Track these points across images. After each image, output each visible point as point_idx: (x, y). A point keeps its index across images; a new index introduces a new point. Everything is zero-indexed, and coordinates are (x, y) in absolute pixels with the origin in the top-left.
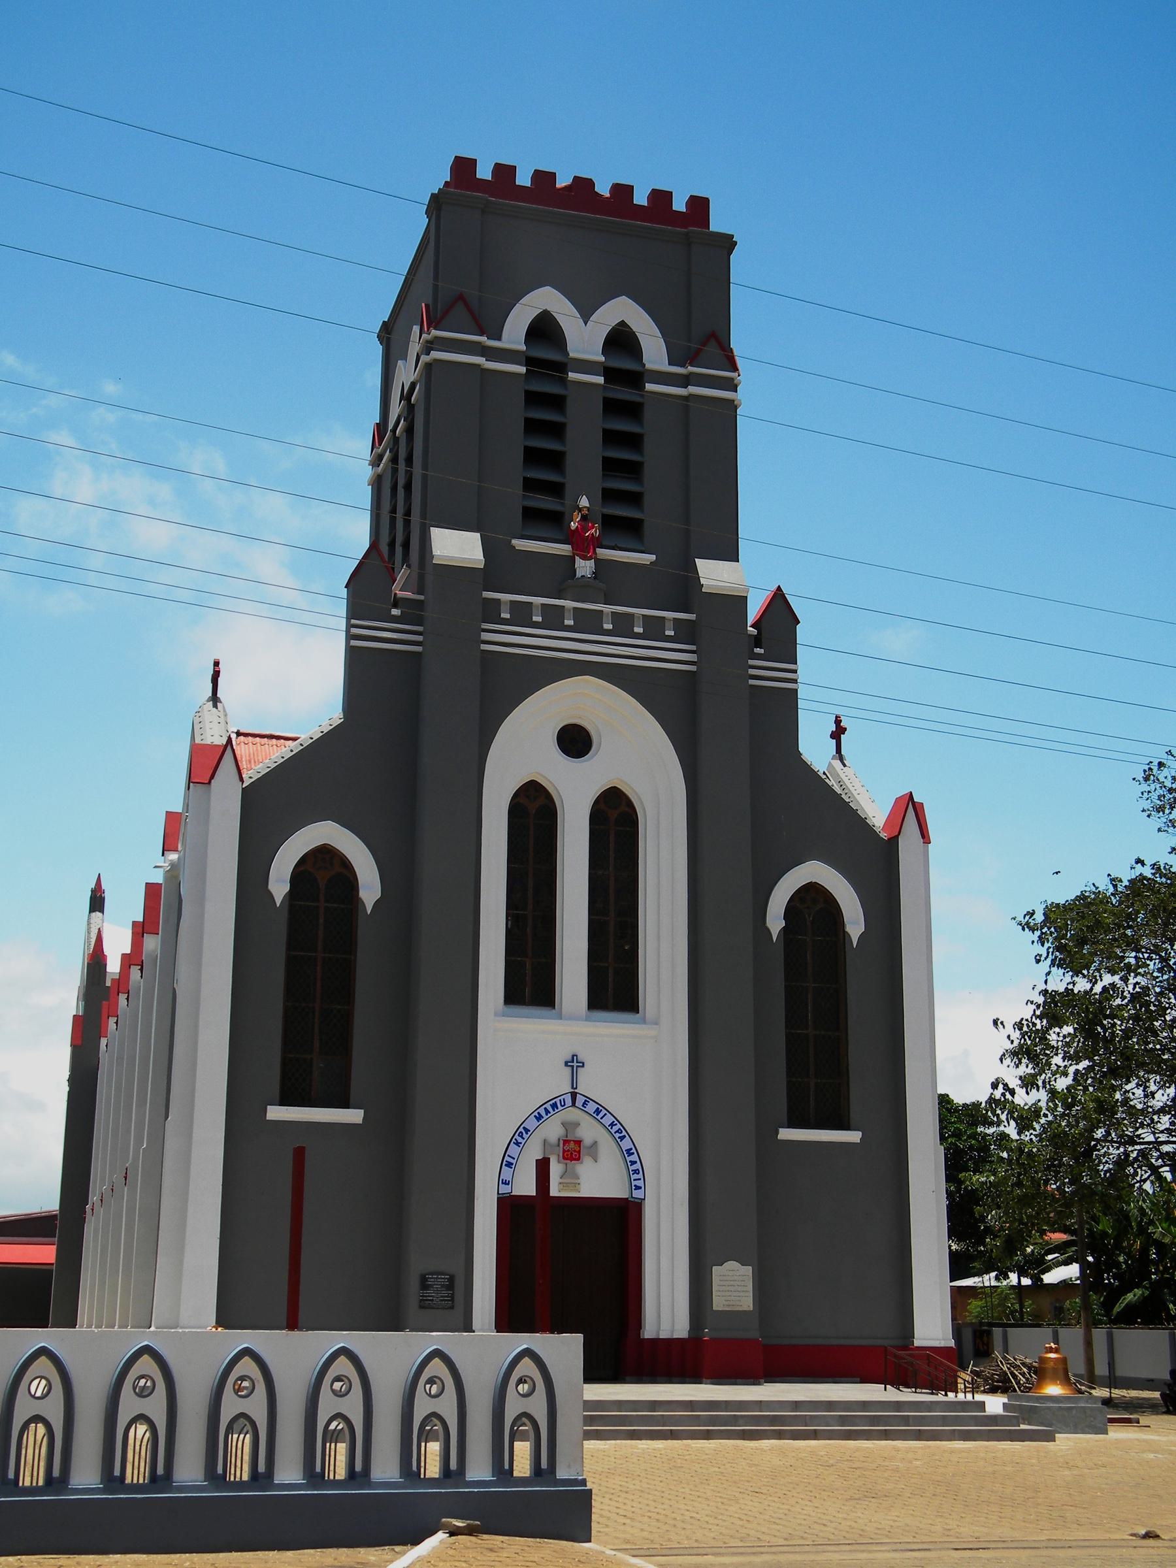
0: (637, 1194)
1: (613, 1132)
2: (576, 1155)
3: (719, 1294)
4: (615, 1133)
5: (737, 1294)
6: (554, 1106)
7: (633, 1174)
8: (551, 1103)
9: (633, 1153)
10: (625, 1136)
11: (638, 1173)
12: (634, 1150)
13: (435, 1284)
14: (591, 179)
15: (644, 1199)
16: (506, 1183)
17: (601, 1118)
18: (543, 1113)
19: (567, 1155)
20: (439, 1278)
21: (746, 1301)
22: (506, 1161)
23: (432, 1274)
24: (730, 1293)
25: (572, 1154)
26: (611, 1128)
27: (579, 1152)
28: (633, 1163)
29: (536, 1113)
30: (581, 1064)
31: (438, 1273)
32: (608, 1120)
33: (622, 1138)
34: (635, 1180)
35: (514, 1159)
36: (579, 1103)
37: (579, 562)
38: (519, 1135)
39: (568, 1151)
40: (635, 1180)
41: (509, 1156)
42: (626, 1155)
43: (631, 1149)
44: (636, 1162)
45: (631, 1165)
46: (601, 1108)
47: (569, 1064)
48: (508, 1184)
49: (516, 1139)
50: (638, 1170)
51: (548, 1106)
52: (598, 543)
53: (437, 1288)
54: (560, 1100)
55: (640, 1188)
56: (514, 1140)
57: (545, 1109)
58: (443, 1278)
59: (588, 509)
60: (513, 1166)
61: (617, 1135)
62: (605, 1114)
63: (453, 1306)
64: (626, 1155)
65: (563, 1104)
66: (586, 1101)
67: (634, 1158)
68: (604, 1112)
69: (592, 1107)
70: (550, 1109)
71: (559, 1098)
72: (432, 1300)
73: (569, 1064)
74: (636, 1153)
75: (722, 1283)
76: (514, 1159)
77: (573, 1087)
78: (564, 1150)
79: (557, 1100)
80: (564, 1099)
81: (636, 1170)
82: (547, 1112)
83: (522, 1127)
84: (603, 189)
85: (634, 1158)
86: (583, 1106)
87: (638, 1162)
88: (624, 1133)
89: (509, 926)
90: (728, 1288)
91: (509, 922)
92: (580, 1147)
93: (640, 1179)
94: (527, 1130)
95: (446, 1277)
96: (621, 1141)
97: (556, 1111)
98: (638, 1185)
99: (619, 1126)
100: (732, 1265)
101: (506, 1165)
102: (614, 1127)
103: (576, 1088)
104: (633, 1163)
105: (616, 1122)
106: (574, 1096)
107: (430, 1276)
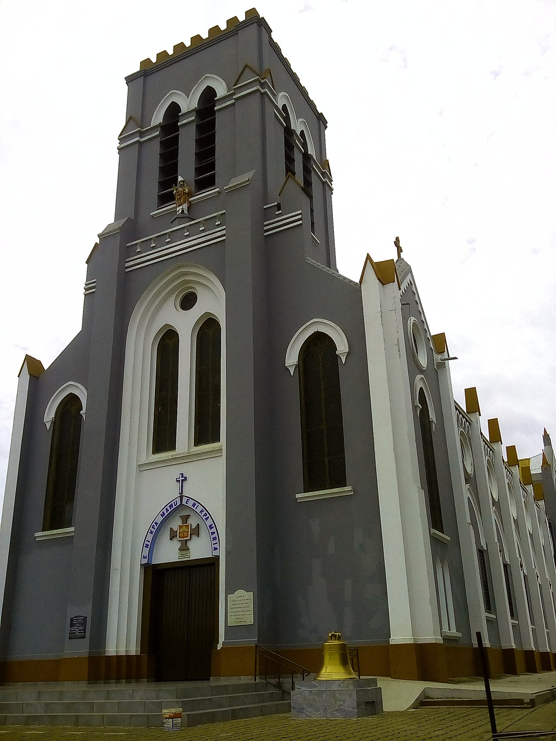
0: (216, 553)
2: (186, 534)
4: (203, 516)
5: (243, 613)
7: (213, 540)
8: (169, 505)
9: (213, 527)
13: (77, 623)
14: (198, 35)
15: (219, 556)
17: (196, 509)
19: (181, 535)
20: (79, 619)
21: (249, 618)
25: (184, 534)
26: (201, 514)
28: (213, 533)
29: (161, 513)
30: (184, 478)
33: (207, 519)
34: (214, 544)
35: (149, 542)
36: (184, 503)
38: (152, 527)
41: (147, 541)
43: (212, 525)
44: (214, 533)
45: (212, 535)
46: (196, 502)
47: (178, 479)
48: (146, 558)
49: (151, 530)
50: (216, 537)
51: (168, 507)
52: (190, 195)
53: (78, 625)
54: (174, 502)
55: (217, 549)
56: (150, 531)
57: (166, 509)
59: (183, 182)
60: (149, 547)
62: (198, 506)
63: (85, 636)
65: (176, 504)
66: (188, 500)
68: (197, 504)
69: (190, 504)
70: (169, 509)
71: (174, 501)
72: (75, 633)
73: (178, 479)
74: (214, 527)
75: (233, 606)
76: (149, 542)
77: (180, 493)
80: (176, 501)
81: (214, 538)
82: (167, 510)
85: (214, 530)
87: (216, 532)
88: (208, 515)
92: (188, 529)
93: (217, 543)
94: (156, 523)
95: (82, 618)
96: (206, 521)
97: (172, 509)
99: (205, 512)
102: (202, 513)
103: (182, 494)
104: (213, 533)
106: (181, 497)
107: (75, 619)
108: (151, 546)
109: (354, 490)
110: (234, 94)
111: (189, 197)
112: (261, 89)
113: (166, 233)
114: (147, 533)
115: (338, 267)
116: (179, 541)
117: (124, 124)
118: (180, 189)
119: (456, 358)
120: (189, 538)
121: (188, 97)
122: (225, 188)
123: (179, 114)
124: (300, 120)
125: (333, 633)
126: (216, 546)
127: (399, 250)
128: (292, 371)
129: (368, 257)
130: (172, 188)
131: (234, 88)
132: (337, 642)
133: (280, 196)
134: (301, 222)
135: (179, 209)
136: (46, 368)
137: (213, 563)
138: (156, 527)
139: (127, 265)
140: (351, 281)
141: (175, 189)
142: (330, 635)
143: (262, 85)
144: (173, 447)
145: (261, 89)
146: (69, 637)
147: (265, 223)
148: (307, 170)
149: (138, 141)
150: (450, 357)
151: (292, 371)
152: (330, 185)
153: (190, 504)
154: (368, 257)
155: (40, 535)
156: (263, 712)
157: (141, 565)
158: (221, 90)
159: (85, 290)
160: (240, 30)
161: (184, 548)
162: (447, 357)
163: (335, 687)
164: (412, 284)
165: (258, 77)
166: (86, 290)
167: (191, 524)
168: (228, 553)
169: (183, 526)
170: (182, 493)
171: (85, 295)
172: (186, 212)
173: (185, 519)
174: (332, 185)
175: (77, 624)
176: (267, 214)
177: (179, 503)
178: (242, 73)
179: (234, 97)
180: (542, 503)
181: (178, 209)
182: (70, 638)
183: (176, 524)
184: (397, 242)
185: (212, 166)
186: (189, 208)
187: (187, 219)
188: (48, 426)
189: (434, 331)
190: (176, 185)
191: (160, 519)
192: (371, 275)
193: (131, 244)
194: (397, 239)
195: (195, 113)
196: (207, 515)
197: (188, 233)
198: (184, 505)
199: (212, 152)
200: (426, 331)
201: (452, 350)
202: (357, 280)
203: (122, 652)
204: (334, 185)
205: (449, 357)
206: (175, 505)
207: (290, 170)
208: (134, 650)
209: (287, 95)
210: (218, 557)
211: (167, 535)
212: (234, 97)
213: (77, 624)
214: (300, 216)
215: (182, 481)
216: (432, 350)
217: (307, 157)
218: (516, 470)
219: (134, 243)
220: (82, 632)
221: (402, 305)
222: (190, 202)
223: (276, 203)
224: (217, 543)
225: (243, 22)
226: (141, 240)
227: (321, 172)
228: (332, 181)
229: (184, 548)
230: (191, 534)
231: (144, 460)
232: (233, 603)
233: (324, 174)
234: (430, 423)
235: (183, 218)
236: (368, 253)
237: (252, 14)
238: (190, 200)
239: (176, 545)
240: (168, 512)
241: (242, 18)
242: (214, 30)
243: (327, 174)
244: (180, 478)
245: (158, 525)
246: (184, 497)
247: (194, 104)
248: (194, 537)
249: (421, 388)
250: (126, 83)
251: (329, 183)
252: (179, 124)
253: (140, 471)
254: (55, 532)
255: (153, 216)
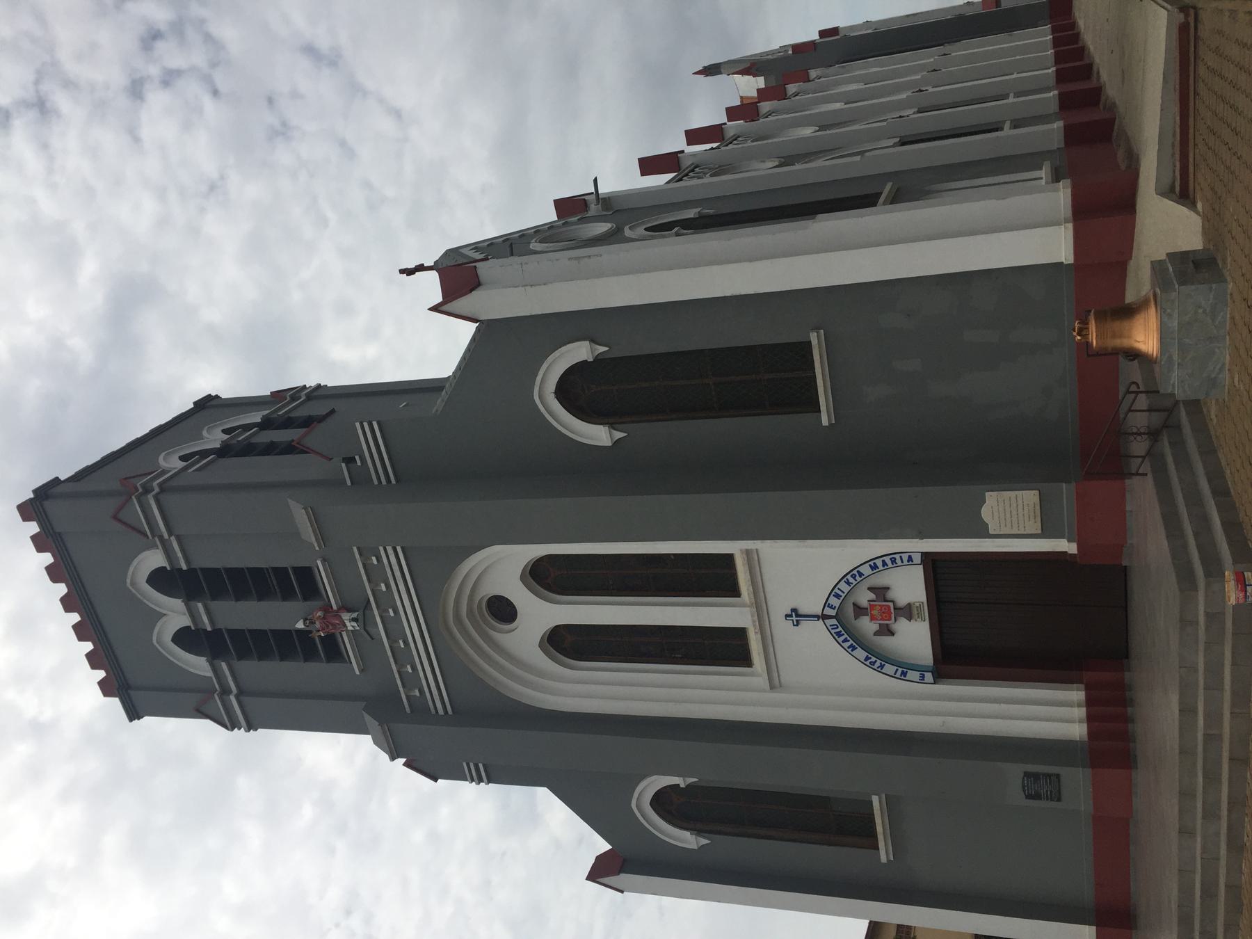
0: (917, 558)
1: (855, 583)
3: (1021, 526)
6: (839, 634)
7: (896, 563)
8: (836, 637)
9: (874, 563)
10: (858, 572)
11: (895, 559)
12: (871, 563)
15: (923, 554)
16: (923, 677)
17: (844, 593)
18: (847, 644)
19: (886, 617)
20: (1028, 784)
21: (1029, 498)
22: (901, 676)
23: (1024, 792)
24: (1020, 515)
27: (880, 605)
28: (884, 564)
29: (850, 650)
30: (794, 614)
31: (1023, 787)
32: (845, 587)
33: (861, 574)
34: (902, 562)
35: (897, 670)
36: (833, 613)
37: (350, 628)
38: (874, 665)
39: (881, 615)
40: (902, 562)
41: (895, 674)
42: (877, 570)
43: (870, 565)
44: (883, 561)
46: (833, 593)
47: (795, 624)
50: (891, 559)
51: (840, 640)
52: (327, 608)
56: (879, 669)
57: (843, 642)
58: (1028, 782)
59: (305, 620)
60: (905, 670)
61: (858, 578)
62: (839, 589)
64: (877, 570)
66: (828, 606)
67: (879, 563)
68: (836, 590)
69: (835, 602)
70: (843, 638)
71: (830, 629)
72: (1051, 792)
75: (1009, 525)
76: (897, 670)
77: (818, 620)
78: (881, 620)
79: (833, 631)
82: (845, 641)
83: (865, 663)
84: (62, 589)
85: (879, 563)
86: (834, 609)
88: (855, 572)
89: (680, 656)
90: (1015, 519)
91: (676, 656)
92: (876, 605)
93: (901, 557)
94: (867, 659)
97: (843, 632)
98: (907, 558)
99: (849, 577)
100: (986, 513)
101: (905, 676)
102: (850, 581)
104: (884, 564)
105: (845, 579)
106: (824, 617)
108: (904, 668)
109: (817, 329)
110: (161, 537)
111: (330, 610)
112: (154, 493)
113: (391, 647)
114: (883, 673)
115: (445, 375)
116: (895, 620)
117: (208, 722)
118: (318, 625)
119: (595, 180)
120: (891, 605)
121: (165, 615)
122: (317, 549)
123: (193, 628)
124: (205, 433)
125: (1075, 334)
126: (905, 557)
127: (421, 268)
128: (619, 435)
129: (435, 309)
130: (313, 640)
131: (151, 538)
132: (1092, 326)
133: (331, 459)
134: (375, 424)
135: (350, 626)
136: (611, 847)
137: (932, 563)
138: (873, 659)
139: (441, 712)
140: (473, 339)
141: (318, 634)
142: (1079, 338)
143: (147, 490)
144: (741, 633)
145: (154, 493)
146: (1057, 801)
147: (376, 482)
148: (288, 423)
149: (237, 697)
150: (593, 190)
151: (619, 435)
152: (311, 389)
153: (835, 602)
154: (435, 309)
155: (884, 854)
156: (1209, 450)
157: (934, 683)
158: (154, 559)
159: (481, 784)
160: (52, 529)
161: (907, 612)
162: (593, 197)
163: (1174, 324)
164: (476, 247)
165: (133, 497)
166: (480, 780)
167: (869, 601)
168: (922, 535)
169: (871, 614)
170: (817, 617)
171: (489, 781)
172: (355, 615)
173: (859, 611)
174: (310, 387)
175: (1036, 789)
176: (361, 479)
177: (834, 621)
178: (125, 523)
179: (166, 536)
180: (813, 73)
181: (350, 628)
182: (1059, 800)
183: (868, 626)
184: (409, 272)
185: (281, 572)
186: (349, 610)
187: (367, 612)
188: (704, 841)
189: (551, 216)
190: (310, 632)
191: (861, 654)
192: (461, 304)
193: (407, 706)
194: (402, 271)
195: (192, 603)
196: (854, 574)
197: (391, 610)
198: (837, 613)
199: (257, 573)
200: (551, 226)
201: (581, 187)
202: (471, 328)
203: (1081, 712)
204: (311, 383)
205: (592, 193)
206: (838, 627)
207: (290, 449)
208: (1077, 694)
209: (164, 454)
210: (924, 556)
211: (886, 641)
212: (166, 536)
213: (1036, 789)
214: (366, 425)
215: (797, 615)
216: (582, 218)
217: (266, 424)
218: (765, 106)
219: (405, 700)
220: (1050, 779)
221: (513, 255)
222: (339, 609)
223: (343, 465)
224: (901, 557)
225: (40, 525)
226: (401, 689)
227: (289, 403)
228: (305, 386)
229: (907, 612)
230: (886, 601)
231: (761, 681)
232: (1003, 525)
233: (293, 399)
234: (701, 217)
235: (365, 620)
236: (428, 309)
237: (27, 511)
238: (335, 607)
239: (902, 625)
240: (849, 638)
241: (33, 528)
242: (54, 573)
243: (295, 393)
244: (793, 620)
245: (870, 656)
246: (825, 613)
247: (178, 604)
248: (890, 595)
249: (646, 229)
250: (139, 719)
251: (309, 390)
252: (209, 629)
253: (781, 686)
254: (879, 829)
255: (362, 671)
